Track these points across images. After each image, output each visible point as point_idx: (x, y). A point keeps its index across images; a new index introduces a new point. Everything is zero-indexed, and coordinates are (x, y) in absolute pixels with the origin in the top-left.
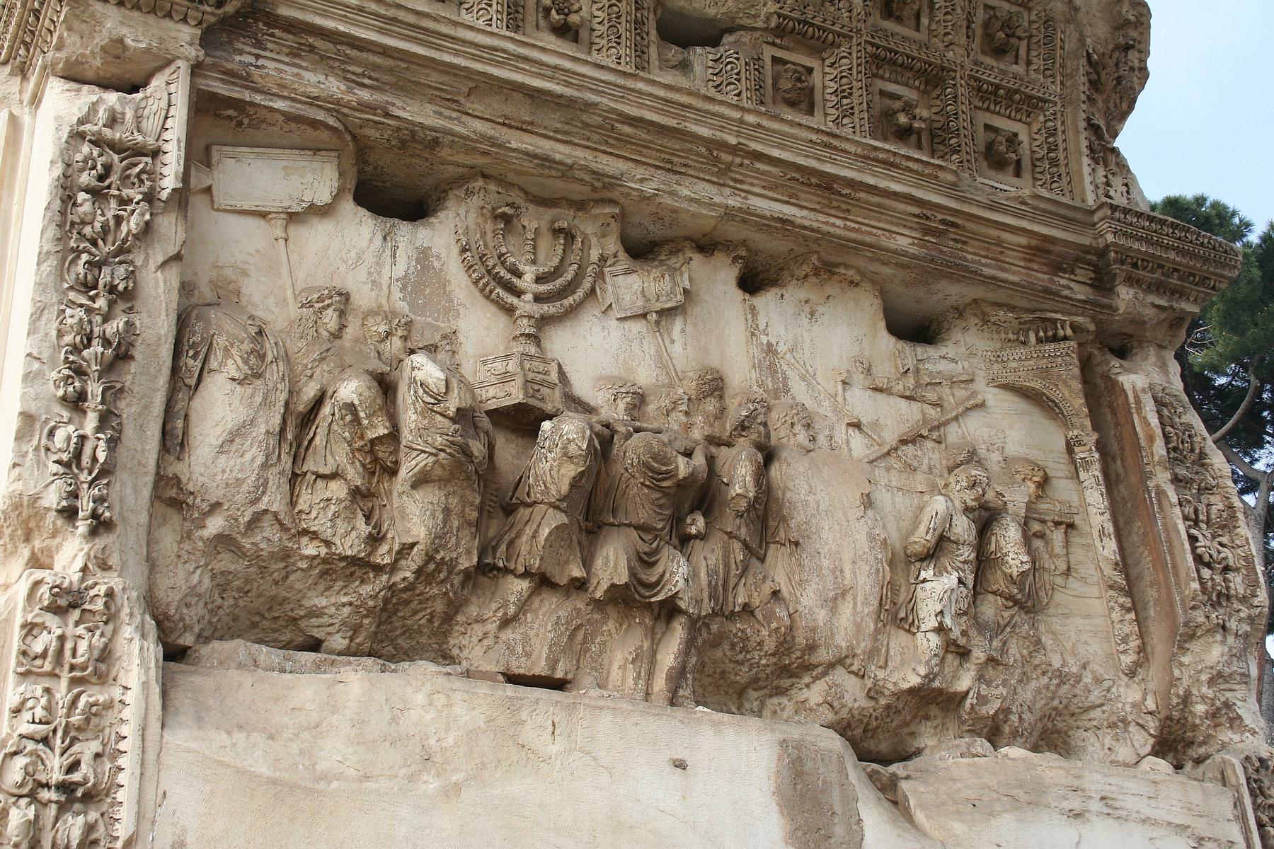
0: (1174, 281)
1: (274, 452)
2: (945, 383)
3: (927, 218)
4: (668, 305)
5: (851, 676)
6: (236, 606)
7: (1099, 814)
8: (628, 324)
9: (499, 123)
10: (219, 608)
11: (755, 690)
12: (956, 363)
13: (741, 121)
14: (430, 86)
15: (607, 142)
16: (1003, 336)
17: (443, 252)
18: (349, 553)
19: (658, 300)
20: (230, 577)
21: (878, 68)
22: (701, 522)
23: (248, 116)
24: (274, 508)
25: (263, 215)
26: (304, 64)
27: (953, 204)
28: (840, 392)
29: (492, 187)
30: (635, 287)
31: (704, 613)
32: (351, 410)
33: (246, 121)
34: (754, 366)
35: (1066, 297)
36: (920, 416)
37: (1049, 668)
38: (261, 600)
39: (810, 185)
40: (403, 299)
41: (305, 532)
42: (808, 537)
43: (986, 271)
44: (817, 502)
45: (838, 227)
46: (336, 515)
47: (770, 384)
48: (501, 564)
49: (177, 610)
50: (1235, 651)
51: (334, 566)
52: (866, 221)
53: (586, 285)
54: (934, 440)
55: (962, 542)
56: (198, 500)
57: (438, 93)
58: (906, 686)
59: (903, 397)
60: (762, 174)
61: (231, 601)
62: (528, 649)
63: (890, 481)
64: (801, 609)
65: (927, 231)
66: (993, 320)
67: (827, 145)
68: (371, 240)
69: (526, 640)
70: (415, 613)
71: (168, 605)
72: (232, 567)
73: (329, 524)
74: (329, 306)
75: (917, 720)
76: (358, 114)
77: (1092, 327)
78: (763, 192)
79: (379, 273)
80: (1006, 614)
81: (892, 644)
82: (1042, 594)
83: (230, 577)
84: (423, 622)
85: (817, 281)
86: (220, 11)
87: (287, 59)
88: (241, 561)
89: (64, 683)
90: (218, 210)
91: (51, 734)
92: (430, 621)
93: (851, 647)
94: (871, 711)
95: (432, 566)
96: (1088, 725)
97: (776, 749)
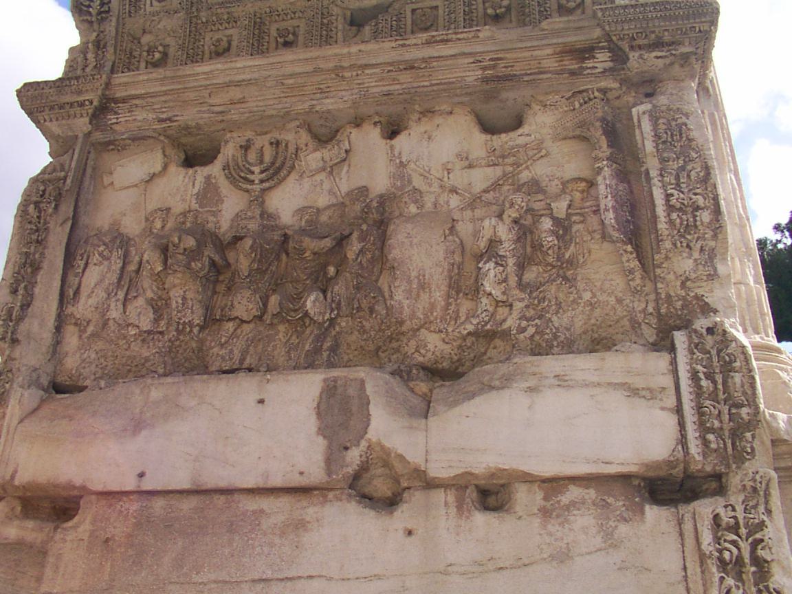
0: (667, 38)
2: (521, 150)
3: (480, 62)
4: (336, 161)
6: (115, 364)
8: (314, 178)
10: (106, 366)
13: (349, 53)
15: (283, 92)
16: (561, 110)
19: (331, 160)
25: (136, 186)
29: (235, 135)
31: (326, 318)
35: (589, 74)
39: (401, 70)
41: (129, 325)
43: (526, 78)
44: (411, 242)
45: (427, 86)
46: (140, 313)
48: (218, 317)
50: (699, 262)
53: (289, 164)
57: (196, 102)
58: (466, 332)
59: (489, 166)
67: (403, 46)
69: (231, 351)
70: (185, 350)
71: (72, 370)
72: (104, 347)
77: (616, 85)
80: (545, 275)
81: (461, 310)
82: (580, 257)
92: (193, 352)
94: (449, 351)
95: (181, 327)
96: (621, 330)
97: (322, 384)
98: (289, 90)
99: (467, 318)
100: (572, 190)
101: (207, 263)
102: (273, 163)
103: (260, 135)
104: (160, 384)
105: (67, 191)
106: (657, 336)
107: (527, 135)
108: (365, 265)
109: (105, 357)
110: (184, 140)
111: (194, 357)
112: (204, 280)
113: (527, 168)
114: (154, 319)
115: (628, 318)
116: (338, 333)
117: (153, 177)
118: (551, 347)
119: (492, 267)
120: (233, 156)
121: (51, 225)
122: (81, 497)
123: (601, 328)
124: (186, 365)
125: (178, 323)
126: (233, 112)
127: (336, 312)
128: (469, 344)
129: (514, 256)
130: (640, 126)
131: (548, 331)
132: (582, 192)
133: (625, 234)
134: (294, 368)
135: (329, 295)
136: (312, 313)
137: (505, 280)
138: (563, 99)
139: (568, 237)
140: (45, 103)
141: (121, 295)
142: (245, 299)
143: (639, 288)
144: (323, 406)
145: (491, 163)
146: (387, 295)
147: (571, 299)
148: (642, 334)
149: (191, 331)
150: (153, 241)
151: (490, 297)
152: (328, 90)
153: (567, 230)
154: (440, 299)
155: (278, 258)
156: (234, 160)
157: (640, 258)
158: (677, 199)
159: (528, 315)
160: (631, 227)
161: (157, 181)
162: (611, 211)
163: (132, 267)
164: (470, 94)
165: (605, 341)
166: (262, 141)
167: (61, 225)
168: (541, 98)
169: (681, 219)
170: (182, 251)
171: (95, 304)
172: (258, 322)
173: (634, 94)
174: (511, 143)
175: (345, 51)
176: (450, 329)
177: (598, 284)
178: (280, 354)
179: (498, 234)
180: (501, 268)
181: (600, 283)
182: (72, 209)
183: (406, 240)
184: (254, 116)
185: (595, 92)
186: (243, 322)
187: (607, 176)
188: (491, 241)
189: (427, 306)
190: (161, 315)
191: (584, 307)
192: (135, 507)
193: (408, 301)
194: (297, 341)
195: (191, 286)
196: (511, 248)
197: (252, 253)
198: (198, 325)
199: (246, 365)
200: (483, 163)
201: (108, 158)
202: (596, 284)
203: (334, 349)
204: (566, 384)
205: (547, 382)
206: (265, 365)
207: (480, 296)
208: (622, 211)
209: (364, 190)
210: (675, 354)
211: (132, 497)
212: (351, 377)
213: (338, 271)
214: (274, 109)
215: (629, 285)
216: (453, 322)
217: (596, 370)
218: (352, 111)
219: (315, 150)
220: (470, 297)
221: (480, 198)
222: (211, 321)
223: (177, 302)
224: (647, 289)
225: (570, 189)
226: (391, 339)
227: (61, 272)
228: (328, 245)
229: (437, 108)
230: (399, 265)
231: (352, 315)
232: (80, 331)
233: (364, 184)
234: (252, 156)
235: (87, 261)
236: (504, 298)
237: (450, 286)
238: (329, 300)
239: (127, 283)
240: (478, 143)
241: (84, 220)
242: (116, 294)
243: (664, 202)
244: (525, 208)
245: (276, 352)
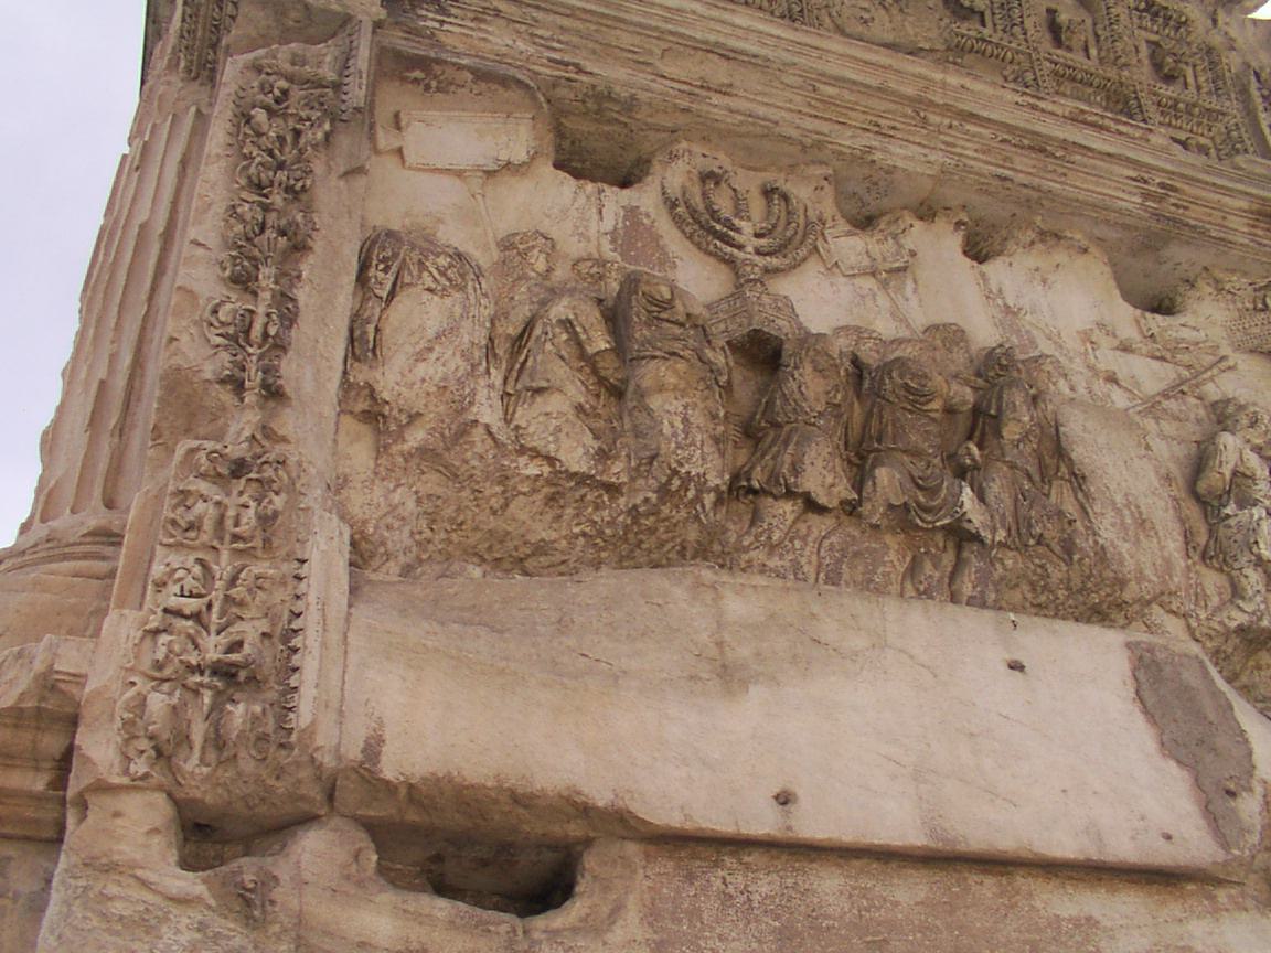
1: (480, 364)
3: (1146, 182)
4: (897, 265)
8: (858, 281)
9: (696, 86)
10: (429, 542)
14: (622, 49)
15: (809, 105)
17: (650, 210)
18: (574, 468)
19: (884, 259)
20: (439, 502)
21: (1059, 84)
22: (975, 450)
23: (435, 77)
24: (485, 419)
25: (459, 174)
26: (490, 29)
27: (1169, 167)
28: (1090, 350)
29: (697, 149)
30: (859, 248)
31: (997, 539)
32: (566, 328)
33: (434, 84)
36: (1175, 376)
38: (479, 535)
39: (1022, 148)
40: (615, 250)
46: (558, 429)
48: (757, 485)
51: (560, 488)
52: (1085, 186)
57: (630, 56)
58: (1233, 625)
60: (974, 136)
61: (443, 535)
64: (1101, 541)
65: (1147, 196)
67: (1034, 108)
68: (574, 200)
70: (662, 544)
72: (440, 491)
73: (551, 439)
74: (533, 247)
75: (1248, 672)
76: (548, 71)
78: (976, 155)
79: (586, 227)
83: (439, 502)
88: (450, 483)
89: (225, 555)
90: (410, 168)
91: (204, 609)
95: (676, 483)
98: (818, 104)
113: (1212, 379)
122: (588, 842)
138: (1250, 288)
144: (1150, 701)
145: (1158, 354)
149: (698, 499)
151: (1259, 569)
154: (1176, 554)
164: (1125, 227)
166: (749, 183)
167: (346, 174)
168: (1220, 275)
171: (439, 375)
175: (938, 76)
176: (1203, 616)
184: (753, 124)
188: (1235, 473)
189: (1159, 562)
192: (765, 885)
193: (1127, 545)
198: (716, 489)
200: (1144, 350)
211: (746, 859)
212: (1176, 649)
229: (1069, 235)
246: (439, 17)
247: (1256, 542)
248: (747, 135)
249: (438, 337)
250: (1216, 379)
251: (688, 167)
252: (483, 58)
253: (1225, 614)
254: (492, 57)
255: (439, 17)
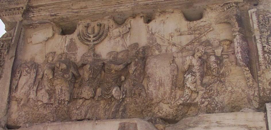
2: (202, 28)
5: (165, 104)
6: (32, 117)
7: (215, 126)
8: (116, 40)
10: (29, 118)
11: (144, 112)
12: (206, 22)
15: (103, 4)
18: (45, 102)
19: (123, 32)
23: (34, 26)
29: (83, 21)
31: (121, 98)
33: (34, 27)
34: (147, 39)
37: (227, 91)
38: (37, 115)
42: (152, 74)
44: (156, 66)
46: (43, 96)
47: (151, 42)
48: (75, 98)
49: (16, 120)
53: (105, 33)
54: (197, 42)
55: (195, 65)
56: (19, 99)
57: (66, 8)
58: (179, 104)
62: (81, 114)
63: (182, 55)
66: (213, 8)
69: (81, 112)
70: (62, 111)
71: (14, 119)
72: (28, 110)
79: (62, 47)
80: (212, 80)
81: (177, 94)
82: (227, 72)
83: (28, 112)
84: (64, 113)
85: (163, 15)
86: (23, 10)
87: (38, 13)
90: (33, 45)
93: (162, 97)
94: (172, 111)
95: (60, 102)
96: (244, 103)
98: (105, 3)
99: (180, 98)
100: (223, 45)
101: (71, 75)
102: (98, 33)
103: (92, 21)
104: (51, 125)
105: (12, 45)
106: (259, 105)
107: (205, 22)
108: (137, 76)
109: (28, 114)
110: (61, 24)
111: (65, 114)
112: (70, 82)
113: (205, 35)
114: (49, 98)
115: (247, 98)
116: (126, 104)
117: (48, 39)
118: (215, 110)
119: (190, 77)
120: (82, 30)
121: (6, 59)
123: (236, 102)
124: (62, 117)
125: (59, 100)
126: (82, 12)
127: (125, 95)
128: (180, 109)
129: (199, 72)
130: (252, 18)
131: (213, 103)
132: (227, 45)
133: (245, 63)
134: (108, 119)
135: (122, 88)
136: (115, 96)
137: (195, 82)
139: (222, 64)
140: (3, 8)
141: (35, 88)
142: (87, 90)
143: (251, 85)
145: (190, 33)
146: (146, 88)
147: (223, 90)
148: (253, 104)
149: (64, 103)
150: (48, 65)
151: (189, 89)
152: (122, 3)
153: (221, 61)
154: (168, 90)
155: (101, 73)
156: (82, 32)
157: (252, 73)
158: (267, 48)
159: (205, 96)
160: (248, 60)
161: (50, 40)
162: (240, 53)
163: (40, 77)
165: (237, 107)
166: (94, 24)
167: (10, 59)
168: (210, 6)
169: (269, 56)
170: (60, 70)
172: (92, 99)
173: (249, 5)
174: (198, 25)
176: (172, 103)
177: (234, 84)
178: (101, 113)
179: (193, 63)
180: (194, 77)
181: (235, 83)
182: (15, 52)
183: (154, 66)
184: (90, 14)
185: (233, 3)
186: (86, 99)
187: (238, 39)
188: (189, 66)
189: (163, 93)
190: (52, 97)
191: (228, 93)
193: (155, 91)
194: (109, 107)
195: (64, 85)
196: (198, 69)
197: (89, 71)
198: (67, 101)
199: (87, 117)
200: (186, 33)
201: (30, 31)
202: (233, 84)
203: (124, 111)
204: (221, 125)
205: (213, 124)
206: (95, 117)
207: (185, 88)
208: (244, 53)
209: (136, 45)
210: (266, 113)
212: (131, 122)
213: (125, 78)
214: (99, 11)
215: (247, 84)
216: (174, 100)
217: (233, 119)
218: (132, 12)
219: (116, 28)
220: (181, 89)
221: (185, 48)
222: (73, 99)
223: (58, 91)
224: (255, 86)
225: (223, 44)
226: (148, 106)
227: (10, 79)
228: (122, 67)
229: (167, 10)
230: (151, 76)
231: (131, 97)
232: (18, 103)
233: (137, 42)
234: (90, 31)
235: (21, 74)
236: (195, 90)
237: (172, 84)
238: (122, 90)
239: (38, 83)
240: (184, 25)
241: (19, 57)
242: (33, 88)
243: (262, 50)
244: (204, 52)
245: (100, 112)
246: (33, 14)
247: (186, 84)
248: (91, 16)
249: (24, 84)
250: (206, 35)
251: (82, 25)
252: (39, 20)
253: (178, 102)
254: (41, 19)
255: (33, 14)
